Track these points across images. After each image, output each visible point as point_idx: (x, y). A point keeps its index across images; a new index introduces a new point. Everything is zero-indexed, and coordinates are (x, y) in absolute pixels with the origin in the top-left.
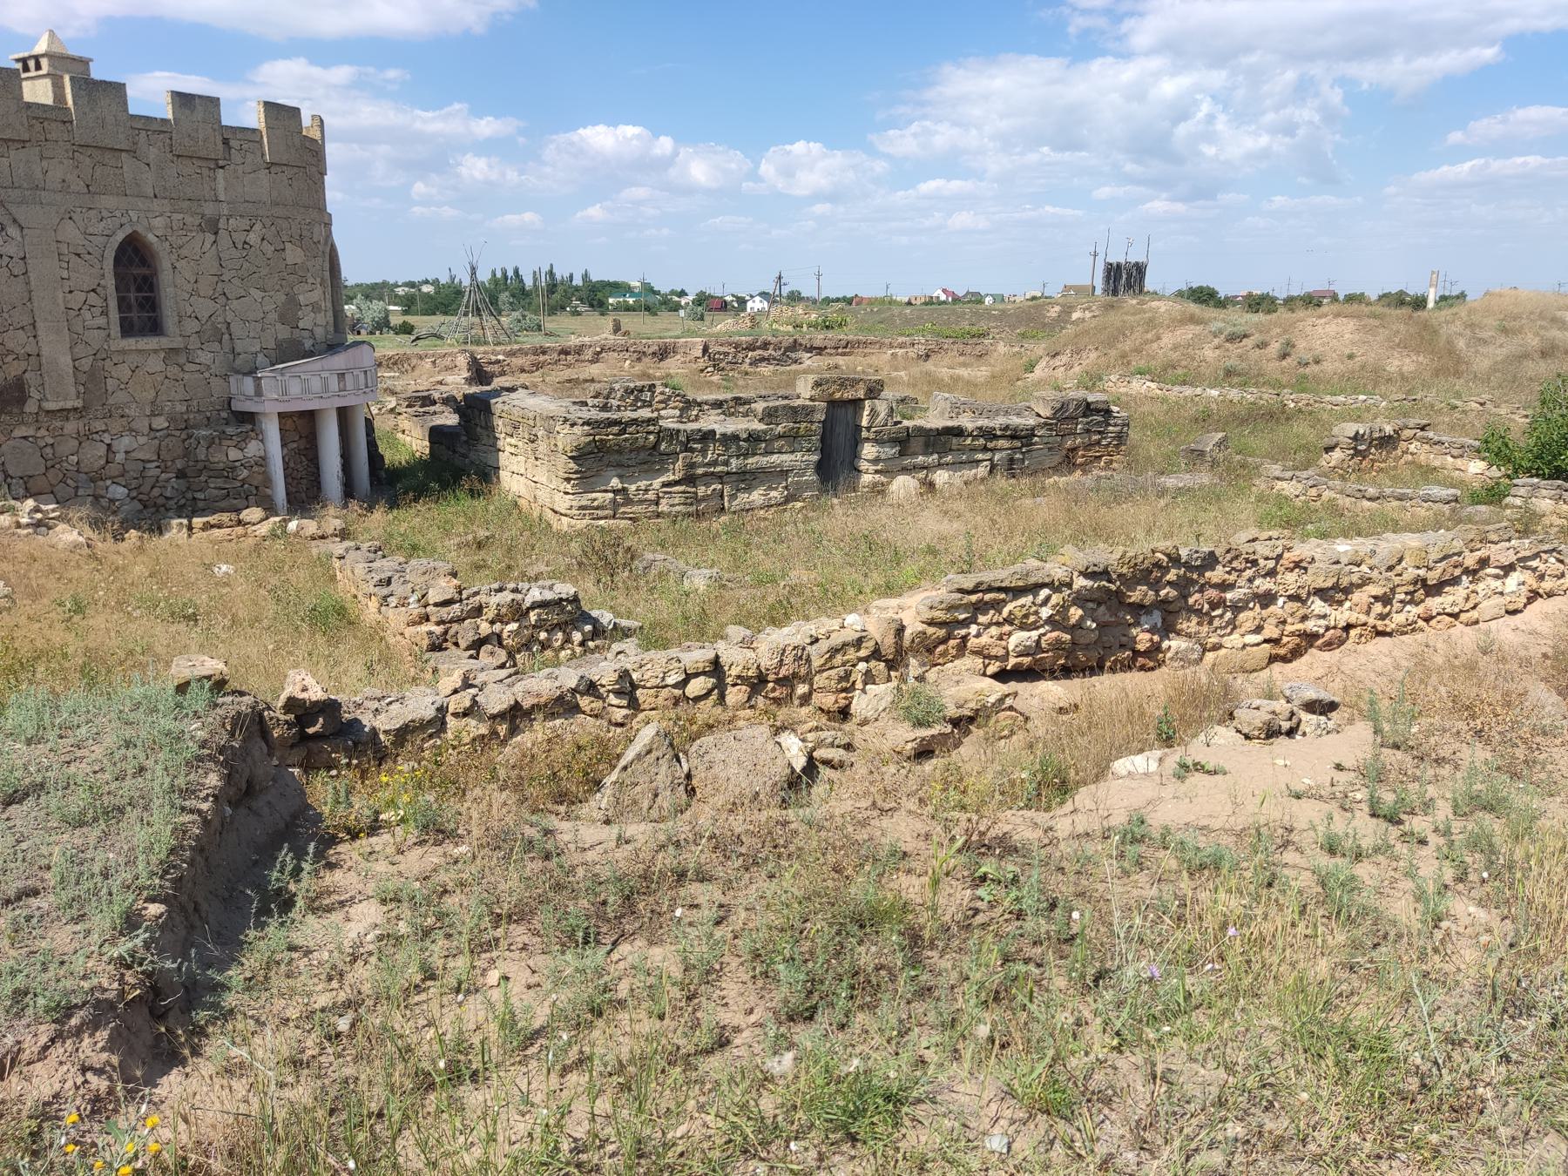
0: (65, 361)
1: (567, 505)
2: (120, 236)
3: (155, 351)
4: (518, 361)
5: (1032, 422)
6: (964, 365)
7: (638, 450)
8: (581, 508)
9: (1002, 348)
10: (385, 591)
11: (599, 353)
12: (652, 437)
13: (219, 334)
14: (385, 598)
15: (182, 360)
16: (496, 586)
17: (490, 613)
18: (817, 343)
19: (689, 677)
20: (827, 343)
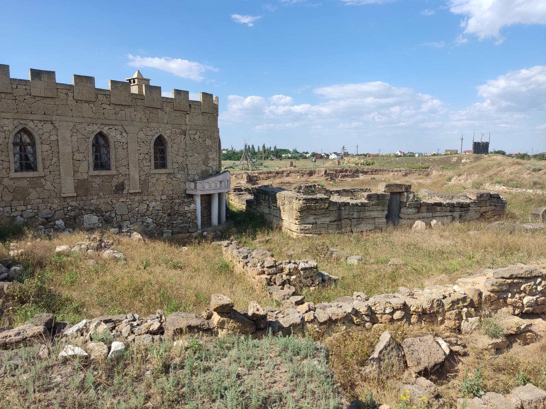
0: (137, 177)
1: (296, 228)
2: (156, 136)
3: (164, 174)
4: (262, 176)
5: (468, 201)
7: (322, 209)
8: (302, 230)
9: (435, 173)
10: (246, 261)
11: (288, 174)
12: (327, 204)
13: (184, 168)
14: (246, 263)
15: (172, 177)
16: (288, 261)
17: (286, 271)
18: (365, 170)
19: (394, 311)
20: (369, 170)
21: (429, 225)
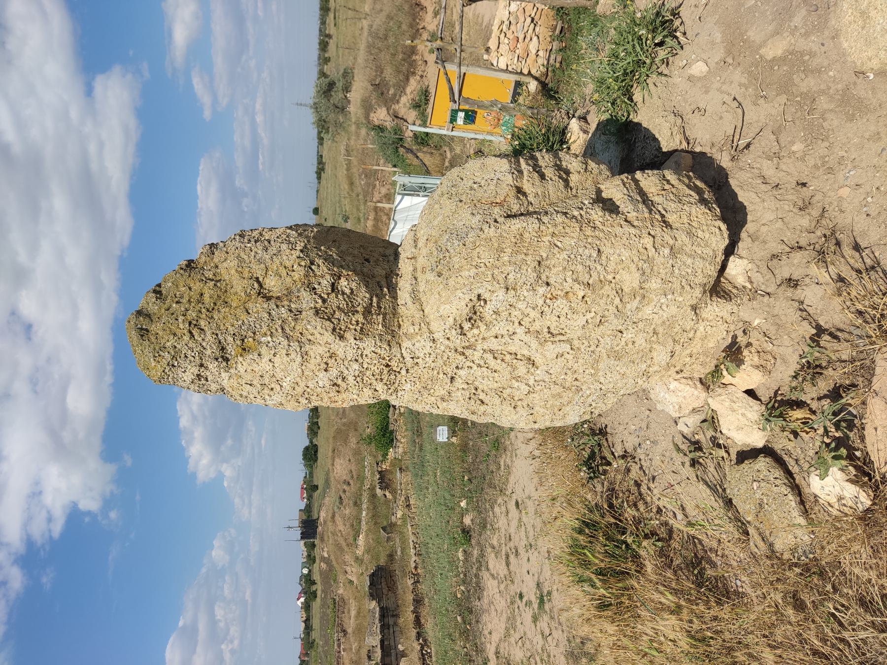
6: (349, 611)
9: (341, 591)
21: (403, 654)
